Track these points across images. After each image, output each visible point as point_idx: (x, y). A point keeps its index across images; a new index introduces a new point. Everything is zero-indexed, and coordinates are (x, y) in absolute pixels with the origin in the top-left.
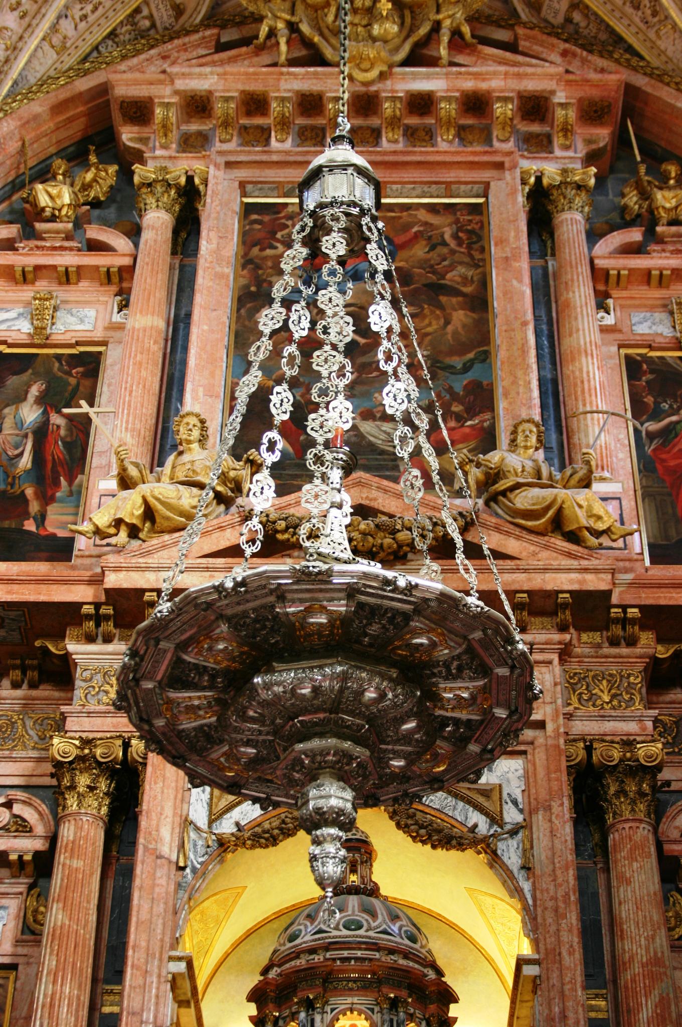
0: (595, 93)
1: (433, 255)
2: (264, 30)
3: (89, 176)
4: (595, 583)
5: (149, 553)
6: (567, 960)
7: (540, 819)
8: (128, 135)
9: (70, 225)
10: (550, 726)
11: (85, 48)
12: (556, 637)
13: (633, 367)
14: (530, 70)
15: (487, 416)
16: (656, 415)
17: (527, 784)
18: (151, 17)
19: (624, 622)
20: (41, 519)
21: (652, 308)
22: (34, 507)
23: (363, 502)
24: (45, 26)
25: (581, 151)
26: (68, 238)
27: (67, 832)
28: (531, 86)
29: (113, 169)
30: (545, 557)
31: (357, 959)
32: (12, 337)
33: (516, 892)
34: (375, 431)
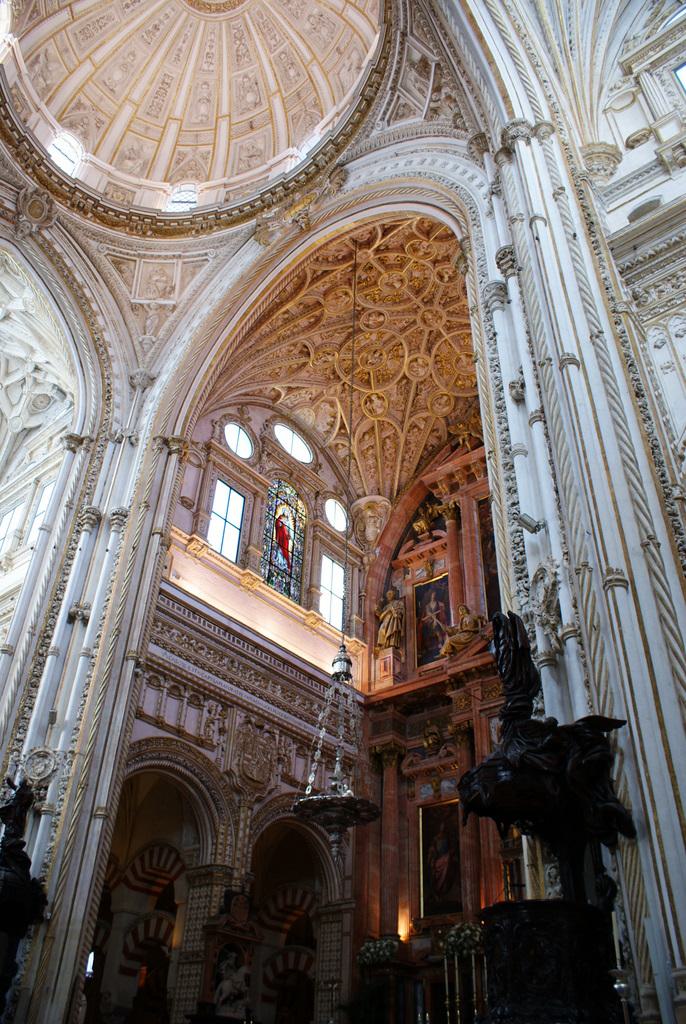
3: (430, 511)
5: (457, 660)
8: (435, 492)
11: (415, 468)
18: (432, 445)
22: (440, 639)
24: (398, 468)
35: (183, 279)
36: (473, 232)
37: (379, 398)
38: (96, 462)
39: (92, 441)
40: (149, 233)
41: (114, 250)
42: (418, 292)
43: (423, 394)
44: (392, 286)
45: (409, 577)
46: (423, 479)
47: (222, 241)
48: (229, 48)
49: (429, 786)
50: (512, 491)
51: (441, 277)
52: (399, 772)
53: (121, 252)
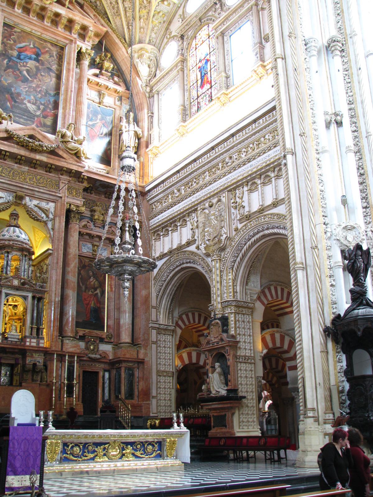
0: (99, 32)
1: (50, 60)
4: (80, 170)
6: (60, 252)
7: (57, 219)
10: (63, 198)
12: (68, 178)
14: (86, 18)
15: (57, 111)
16: (91, 120)
17: (55, 210)
19: (83, 179)
21: (96, 91)
23: (34, 134)
30: (71, 161)
31: (19, 244)
34: (30, 107)
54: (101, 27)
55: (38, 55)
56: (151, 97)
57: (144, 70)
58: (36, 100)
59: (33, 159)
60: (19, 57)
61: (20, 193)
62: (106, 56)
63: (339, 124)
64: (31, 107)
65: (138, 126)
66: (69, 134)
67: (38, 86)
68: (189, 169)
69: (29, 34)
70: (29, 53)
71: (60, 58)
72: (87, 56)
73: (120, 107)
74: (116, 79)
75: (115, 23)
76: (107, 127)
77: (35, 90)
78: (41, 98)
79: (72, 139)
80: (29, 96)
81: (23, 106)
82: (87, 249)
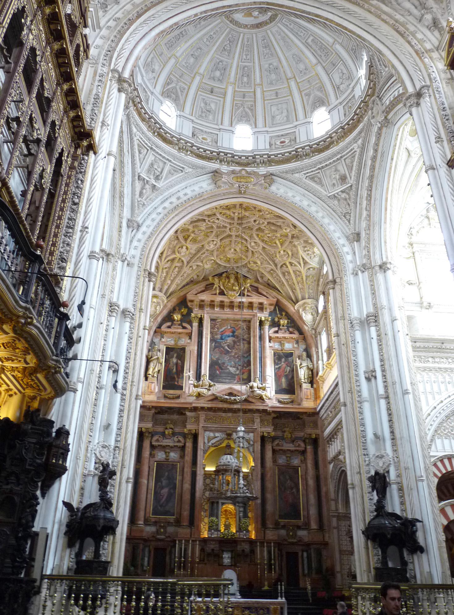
0: (271, 302)
2: (214, 287)
7: (255, 444)
8: (189, 304)
9: (180, 322)
11: (182, 285)
13: (274, 353)
16: (277, 364)
18: (193, 278)
20: (178, 382)
21: (278, 342)
22: (177, 379)
25: (268, 310)
26: (179, 325)
27: (187, 444)
28: (261, 301)
29: (186, 310)
32: (171, 344)
33: (251, 455)
35: (167, 175)
36: (345, 279)
37: (187, 248)
38: (115, 273)
39: (113, 256)
40: (156, 134)
41: (141, 139)
42: (239, 218)
43: (204, 256)
44: (234, 213)
45: (163, 340)
46: (187, 295)
47: (194, 167)
48: (223, 42)
49: (163, 453)
50: (361, 413)
51: (255, 221)
52: (151, 443)
53: (144, 141)
54: (272, 299)
55: (233, 332)
56: (316, 337)
57: (307, 317)
58: (235, 364)
59: (232, 409)
60: (222, 339)
61: (229, 432)
62: (282, 315)
63: (375, 377)
64: (232, 370)
65: (311, 361)
66: (255, 385)
67: (236, 354)
68: (331, 399)
69: (227, 320)
70: (227, 334)
71: (249, 328)
72: (266, 322)
73: (298, 348)
74: (291, 329)
75: (283, 290)
76: (290, 367)
77: (234, 357)
78: (239, 361)
79: (258, 388)
80: (231, 362)
81: (228, 371)
82: (282, 460)
